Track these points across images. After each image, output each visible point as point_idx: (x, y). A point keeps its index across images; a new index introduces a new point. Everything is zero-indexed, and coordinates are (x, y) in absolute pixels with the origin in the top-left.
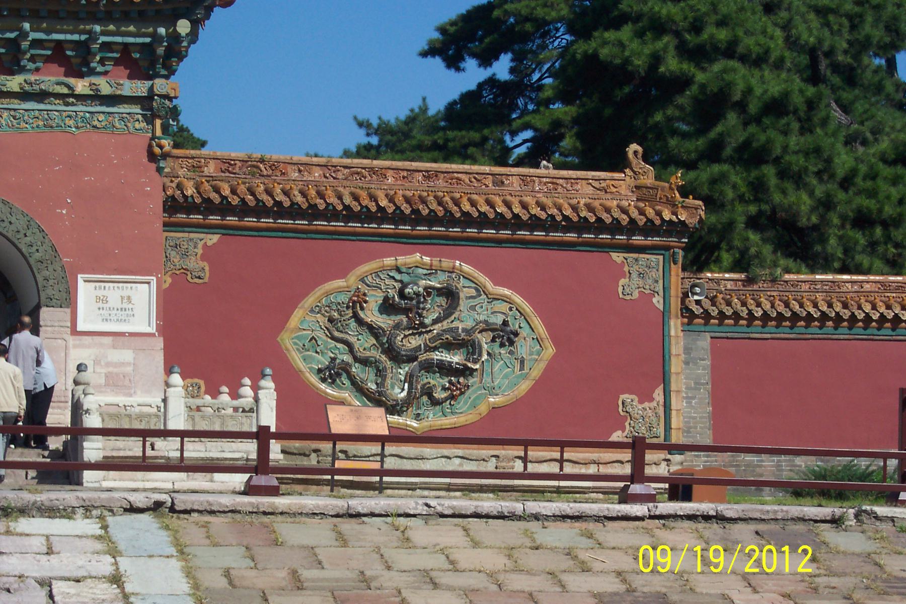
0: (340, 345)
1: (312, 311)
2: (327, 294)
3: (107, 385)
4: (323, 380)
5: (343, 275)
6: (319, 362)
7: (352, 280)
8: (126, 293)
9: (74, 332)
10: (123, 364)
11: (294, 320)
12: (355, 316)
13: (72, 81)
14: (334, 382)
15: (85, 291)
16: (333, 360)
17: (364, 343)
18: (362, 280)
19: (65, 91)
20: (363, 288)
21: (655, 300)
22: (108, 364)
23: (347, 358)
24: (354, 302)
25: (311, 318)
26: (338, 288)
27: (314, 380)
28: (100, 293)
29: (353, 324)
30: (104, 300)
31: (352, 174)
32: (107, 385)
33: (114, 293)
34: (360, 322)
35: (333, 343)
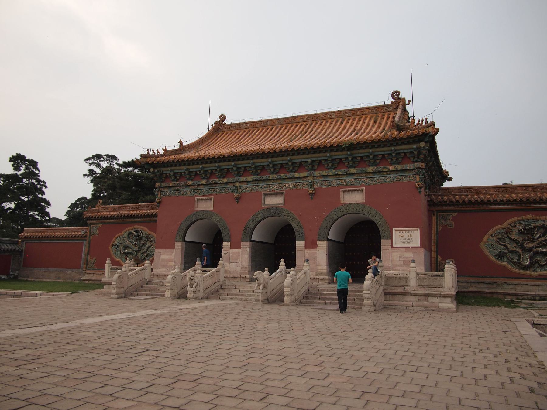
0: (502, 247)
1: (491, 236)
2: (497, 230)
3: (404, 264)
4: (498, 258)
5: (502, 224)
6: (495, 253)
7: (506, 224)
8: (409, 234)
9: (392, 247)
10: (409, 257)
11: (485, 239)
12: (508, 237)
13: (388, 167)
14: (501, 259)
15: (396, 234)
16: (501, 252)
17: (511, 246)
18: (510, 225)
19: (386, 170)
20: (511, 227)
21: (441, 259)
22: (404, 258)
23: (506, 251)
24: (507, 233)
25: (491, 238)
26: (501, 227)
27: (493, 259)
28: (401, 234)
29: (507, 239)
30: (402, 236)
31: (505, 190)
32: (404, 264)
33: (406, 234)
34: (510, 239)
35: (500, 246)
